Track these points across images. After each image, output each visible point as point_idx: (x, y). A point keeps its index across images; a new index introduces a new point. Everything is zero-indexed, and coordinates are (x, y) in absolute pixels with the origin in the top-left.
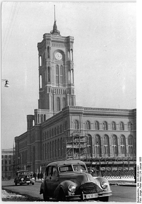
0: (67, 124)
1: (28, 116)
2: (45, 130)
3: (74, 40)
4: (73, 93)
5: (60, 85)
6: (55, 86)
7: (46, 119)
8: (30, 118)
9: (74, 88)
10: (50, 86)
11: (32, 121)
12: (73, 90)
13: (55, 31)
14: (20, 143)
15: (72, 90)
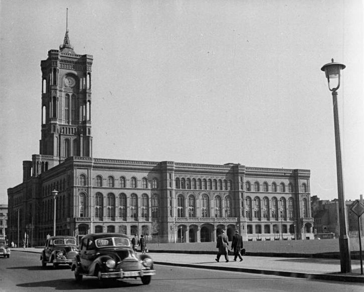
0: (71, 178)
1: (24, 162)
2: (46, 184)
3: (92, 60)
4: (89, 134)
5: (70, 122)
6: (63, 124)
7: (49, 169)
8: (27, 165)
9: (90, 127)
10: (56, 124)
11: (31, 169)
12: (89, 129)
13: (66, 45)
14: (15, 197)
15: (87, 130)
